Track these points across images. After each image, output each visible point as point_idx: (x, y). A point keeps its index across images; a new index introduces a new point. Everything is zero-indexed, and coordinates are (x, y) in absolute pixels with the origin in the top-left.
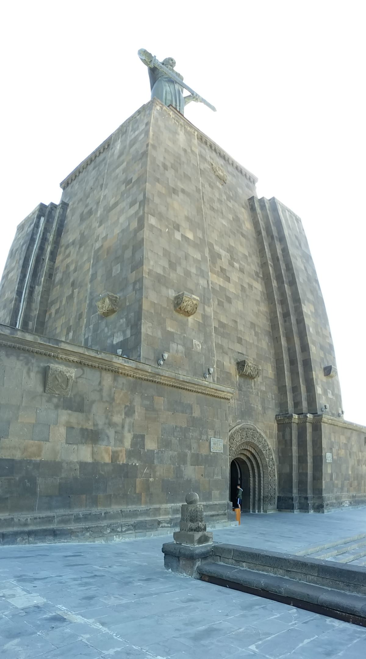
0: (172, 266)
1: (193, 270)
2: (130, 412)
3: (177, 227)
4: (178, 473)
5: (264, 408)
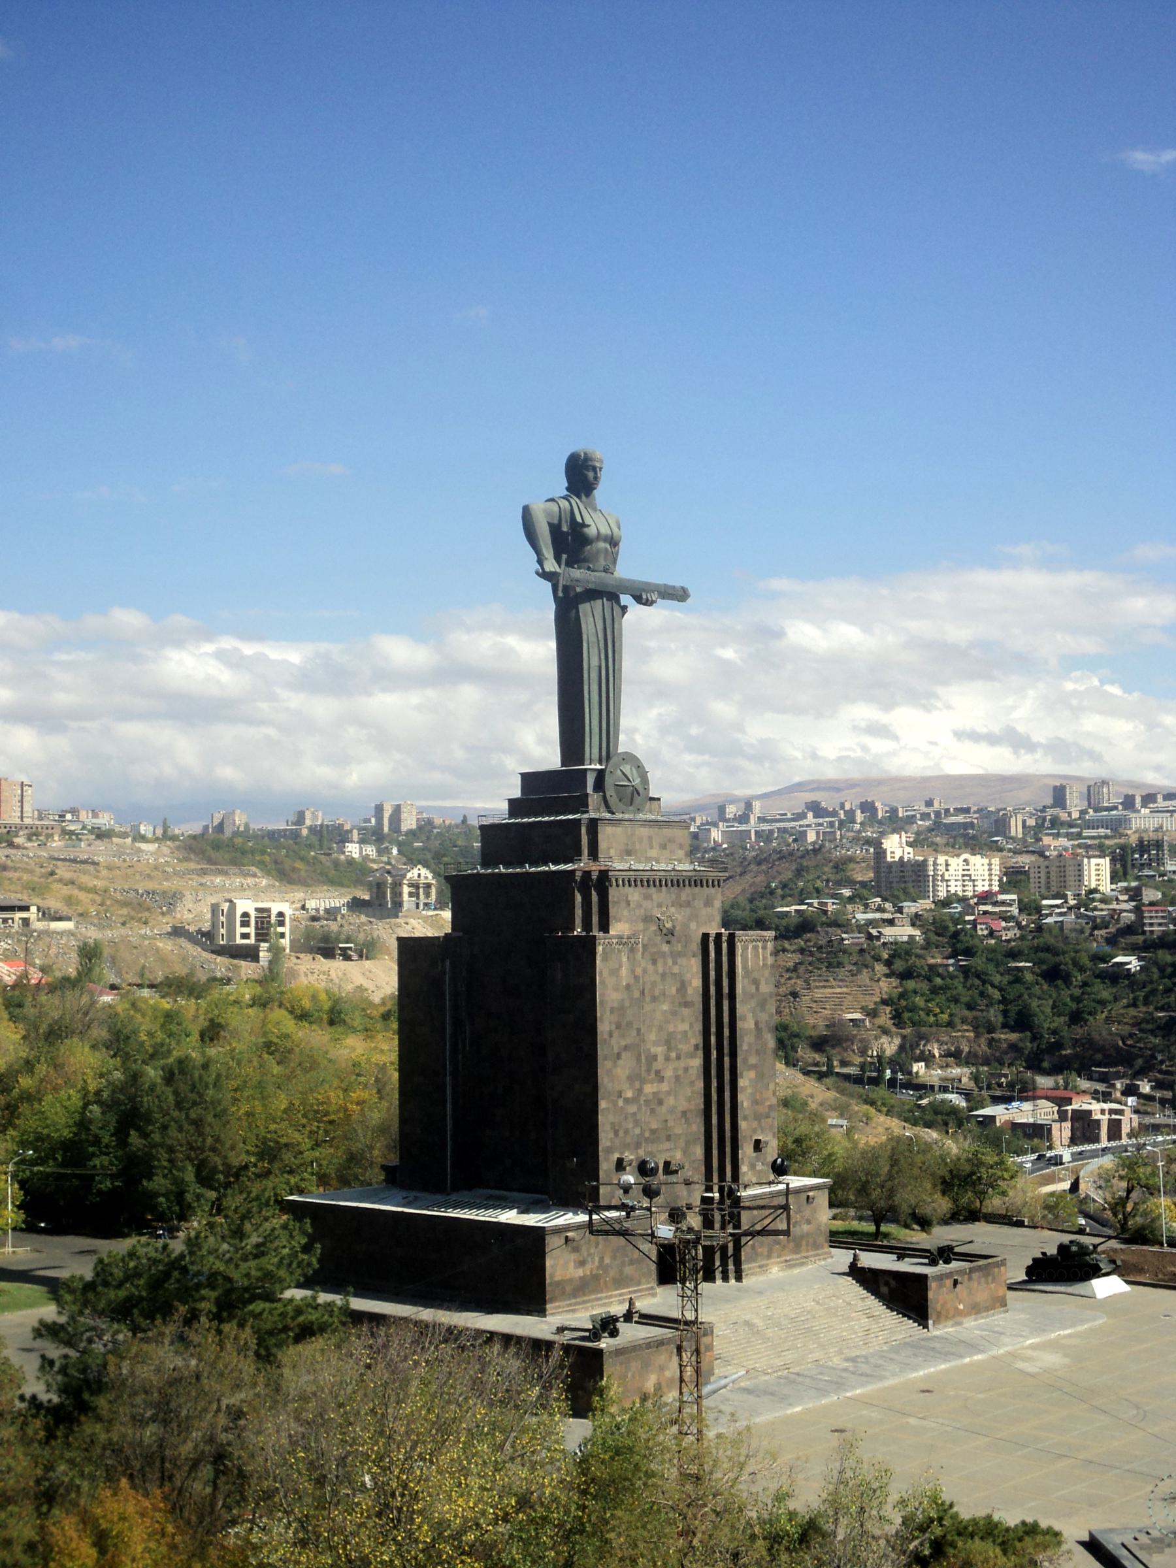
1: (631, 1126)
4: (621, 1272)
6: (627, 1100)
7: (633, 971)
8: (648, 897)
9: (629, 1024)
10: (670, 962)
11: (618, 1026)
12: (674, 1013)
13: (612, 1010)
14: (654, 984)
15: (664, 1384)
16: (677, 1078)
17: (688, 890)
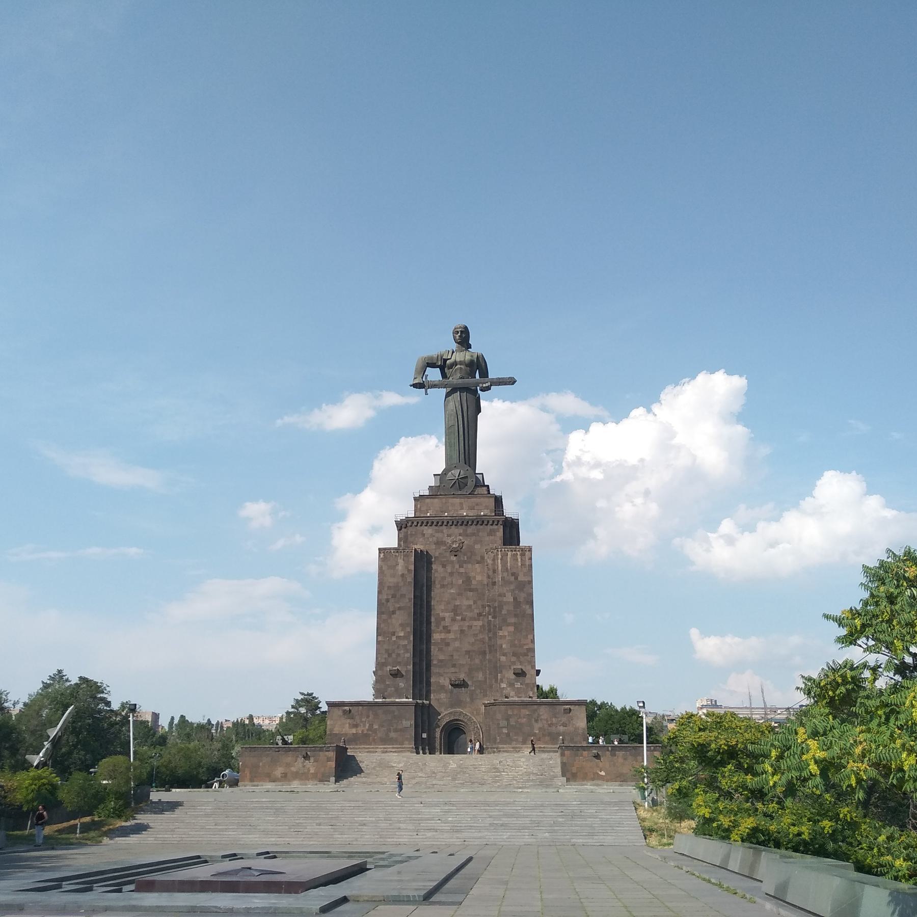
0: (390, 655)
2: (368, 717)
3: (393, 634)
5: (472, 700)
6: (398, 637)
7: (407, 568)
8: (437, 531)
9: (403, 596)
10: (457, 566)
11: (394, 596)
12: (460, 594)
13: (389, 588)
14: (444, 578)
15: (289, 775)
16: (462, 631)
17: (473, 527)
